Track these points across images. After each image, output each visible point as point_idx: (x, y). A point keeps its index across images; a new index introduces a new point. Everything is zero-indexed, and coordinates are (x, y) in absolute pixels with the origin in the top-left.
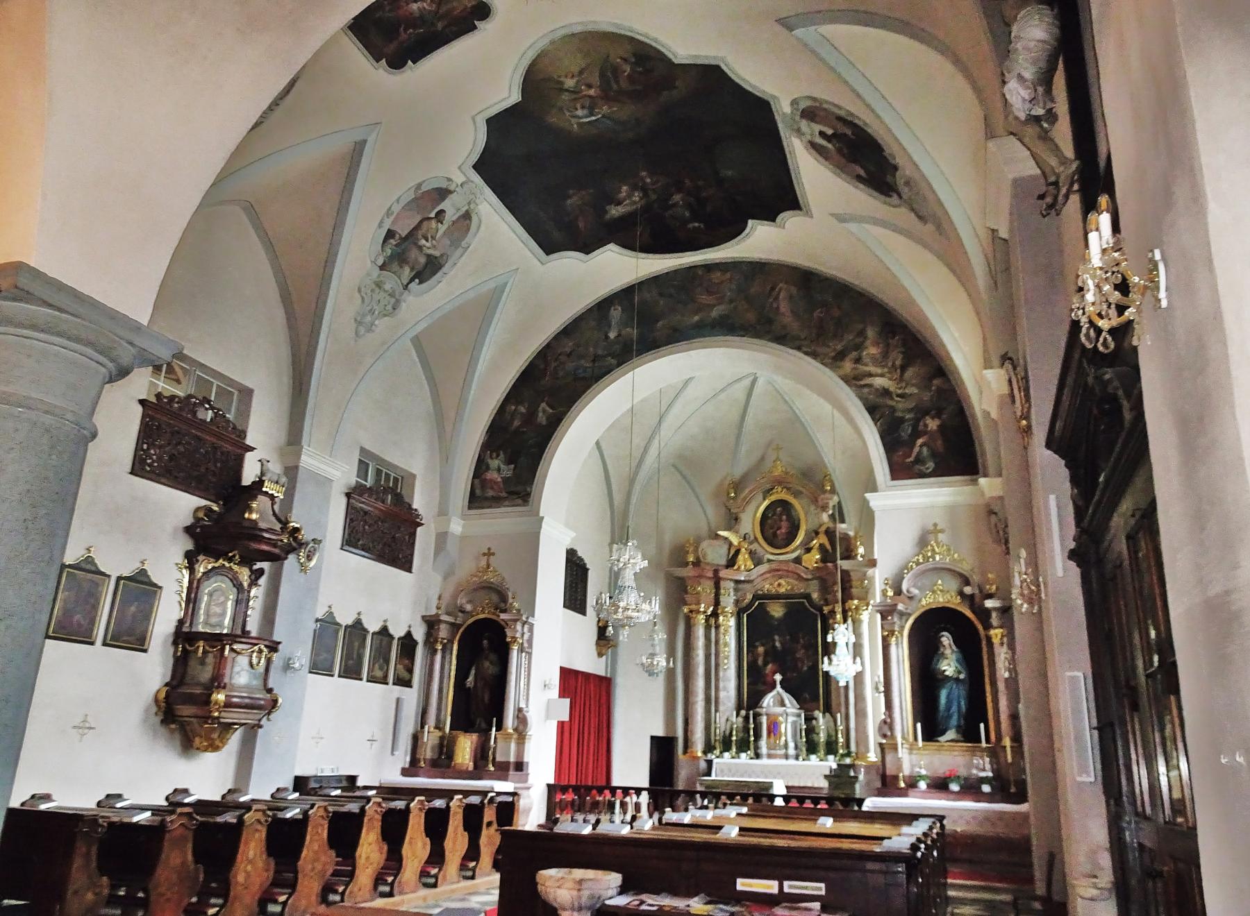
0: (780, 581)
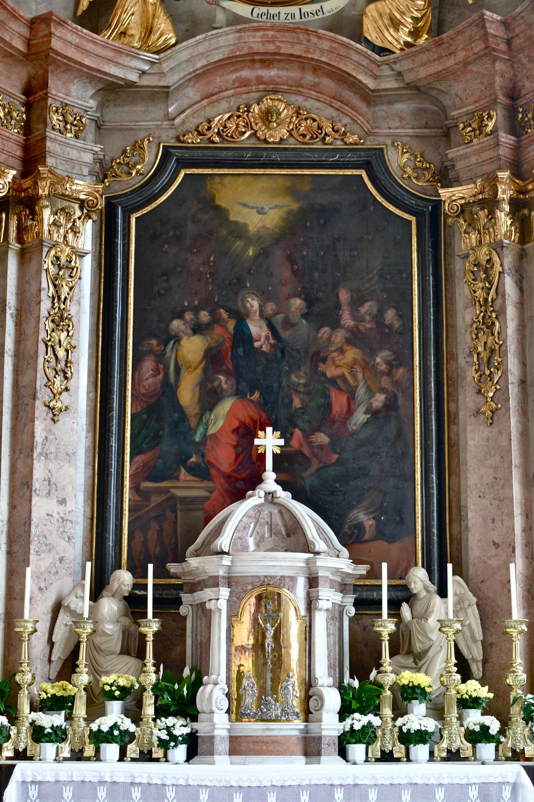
0: (267, 102)
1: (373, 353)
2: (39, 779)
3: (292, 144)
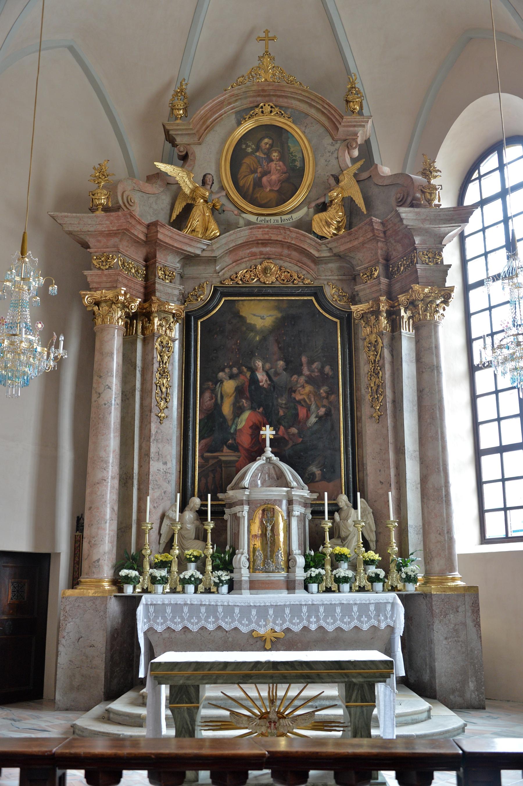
0: (265, 264)
1: (319, 388)
2: (155, 602)
3: (277, 284)
